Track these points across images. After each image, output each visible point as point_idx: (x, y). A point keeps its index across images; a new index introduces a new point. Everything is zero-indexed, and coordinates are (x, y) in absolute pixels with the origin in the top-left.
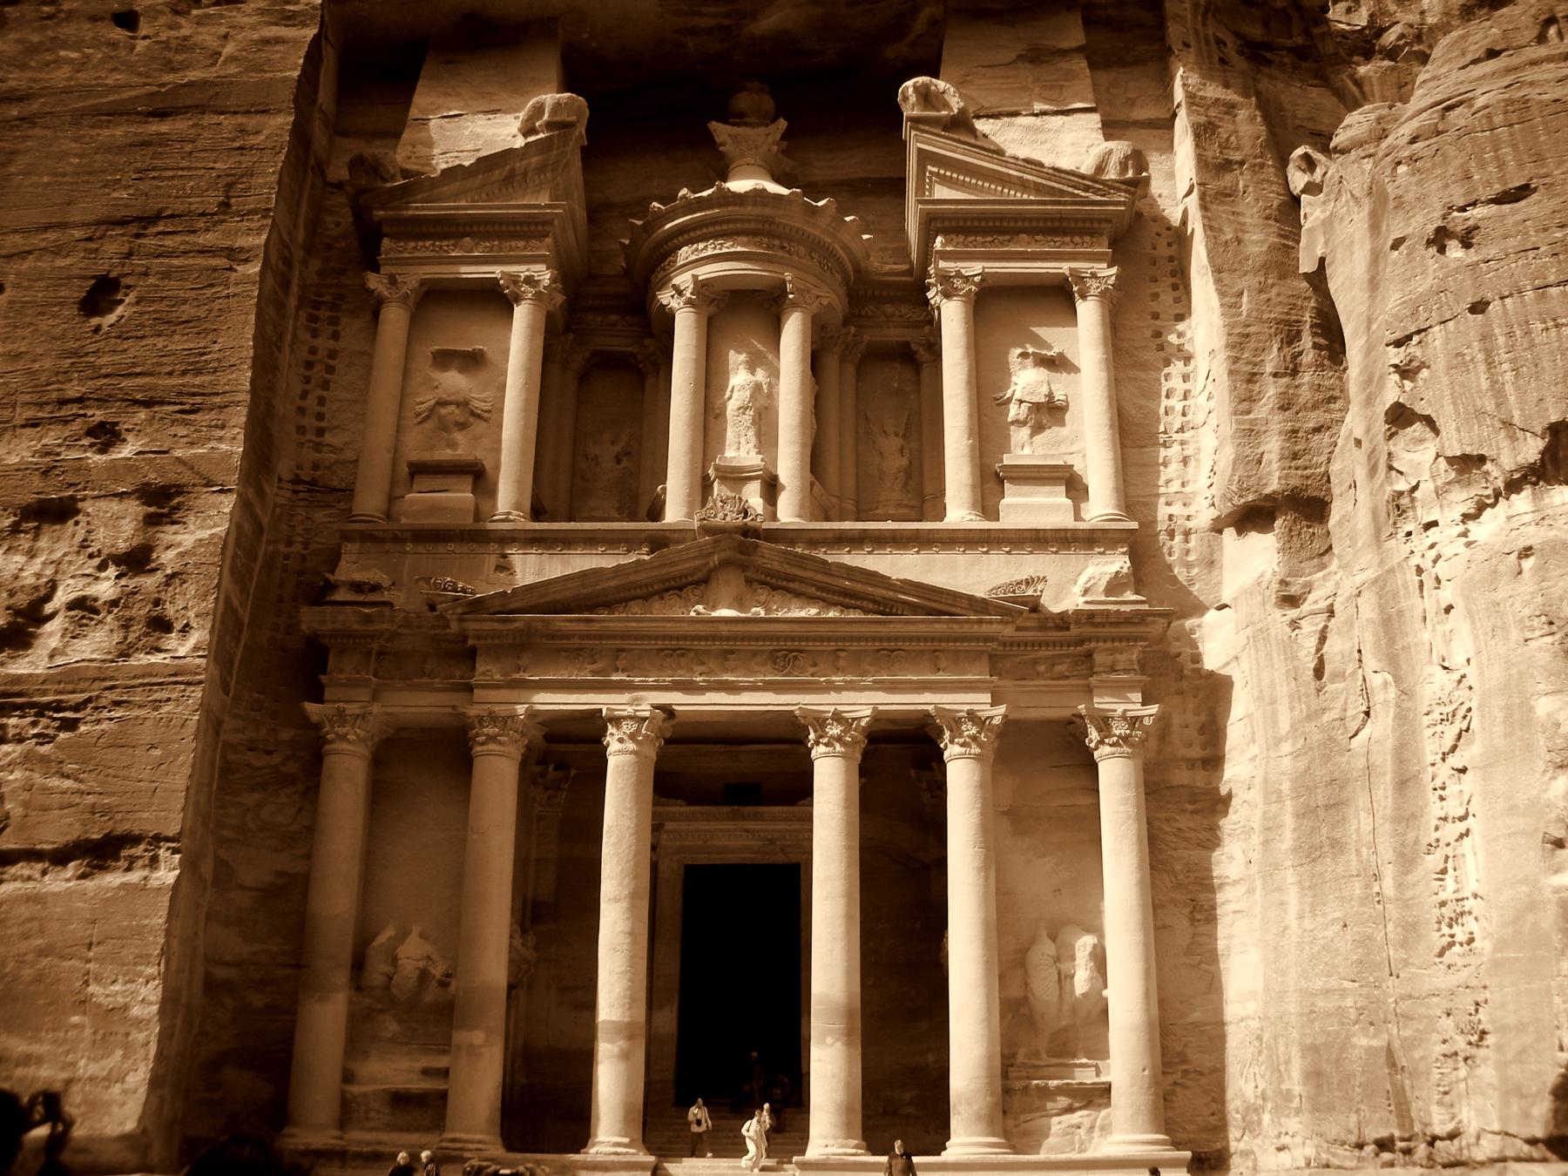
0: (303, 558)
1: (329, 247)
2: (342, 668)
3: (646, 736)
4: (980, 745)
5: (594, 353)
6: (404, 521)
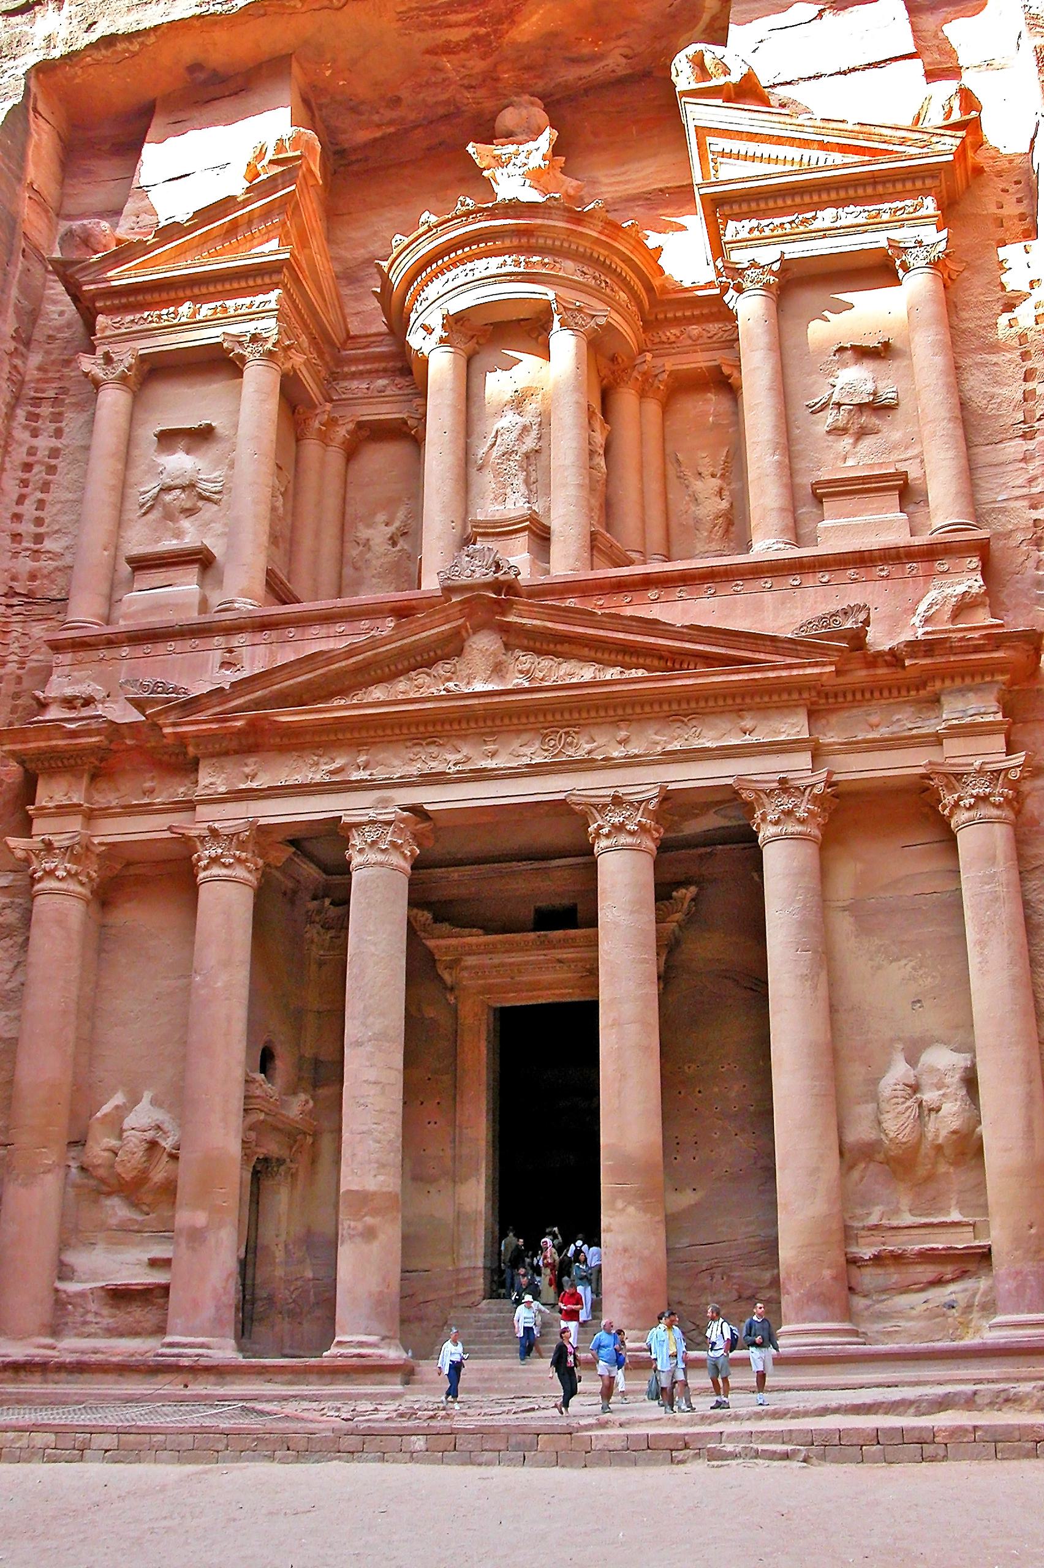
0: (19, 680)
1: (49, 336)
2: (51, 793)
3: (393, 844)
4: (802, 821)
5: (361, 425)
6: (122, 622)
